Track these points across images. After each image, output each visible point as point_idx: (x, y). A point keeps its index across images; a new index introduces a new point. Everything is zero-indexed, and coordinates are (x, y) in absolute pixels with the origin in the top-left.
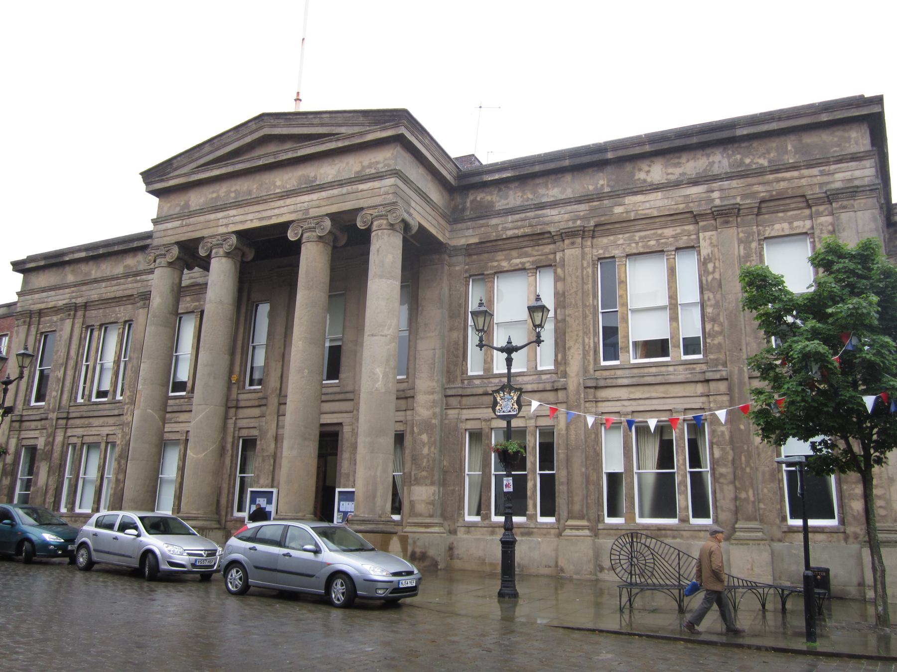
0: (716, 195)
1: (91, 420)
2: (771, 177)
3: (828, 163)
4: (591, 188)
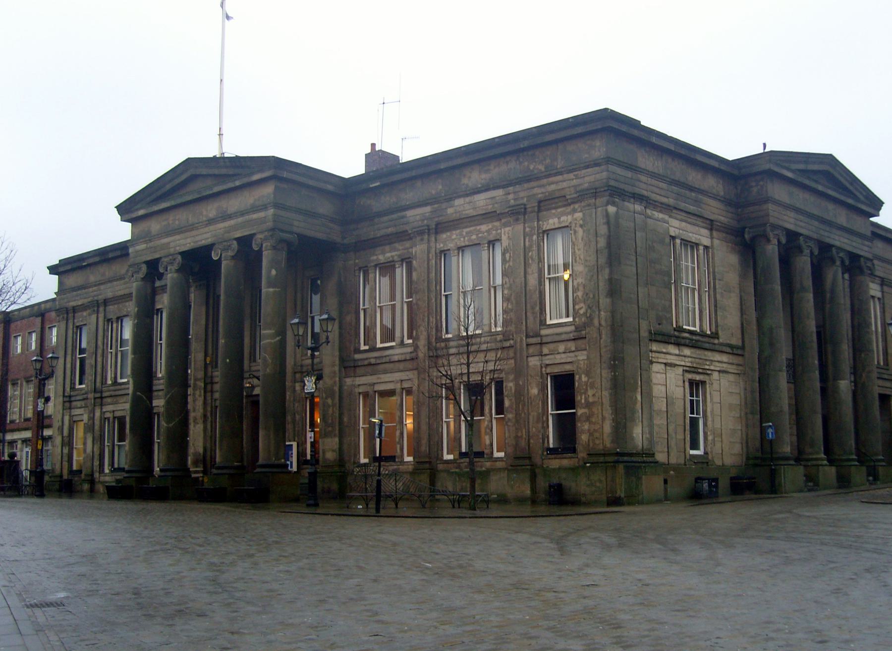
0: (511, 197)
1: (118, 398)
2: (545, 181)
3: (579, 169)
4: (433, 192)
